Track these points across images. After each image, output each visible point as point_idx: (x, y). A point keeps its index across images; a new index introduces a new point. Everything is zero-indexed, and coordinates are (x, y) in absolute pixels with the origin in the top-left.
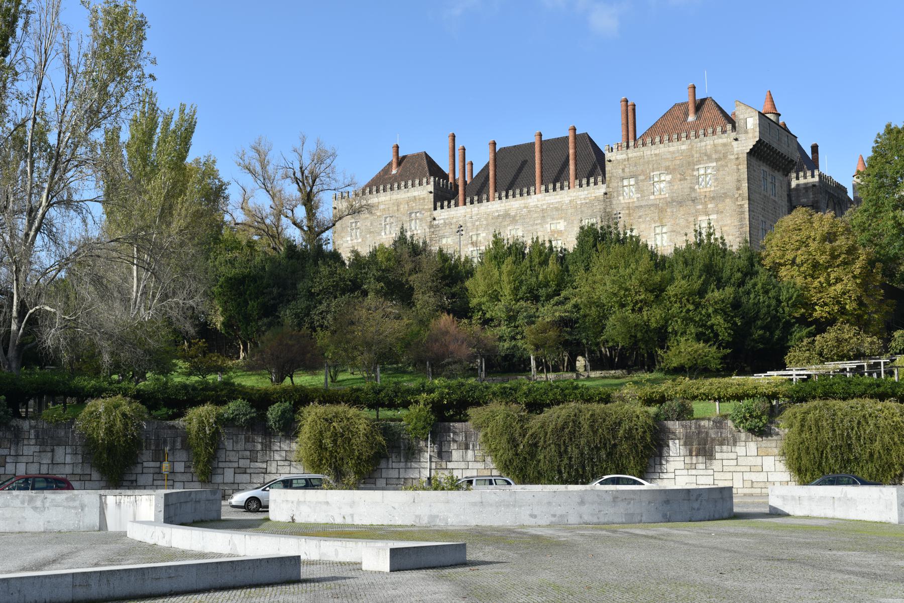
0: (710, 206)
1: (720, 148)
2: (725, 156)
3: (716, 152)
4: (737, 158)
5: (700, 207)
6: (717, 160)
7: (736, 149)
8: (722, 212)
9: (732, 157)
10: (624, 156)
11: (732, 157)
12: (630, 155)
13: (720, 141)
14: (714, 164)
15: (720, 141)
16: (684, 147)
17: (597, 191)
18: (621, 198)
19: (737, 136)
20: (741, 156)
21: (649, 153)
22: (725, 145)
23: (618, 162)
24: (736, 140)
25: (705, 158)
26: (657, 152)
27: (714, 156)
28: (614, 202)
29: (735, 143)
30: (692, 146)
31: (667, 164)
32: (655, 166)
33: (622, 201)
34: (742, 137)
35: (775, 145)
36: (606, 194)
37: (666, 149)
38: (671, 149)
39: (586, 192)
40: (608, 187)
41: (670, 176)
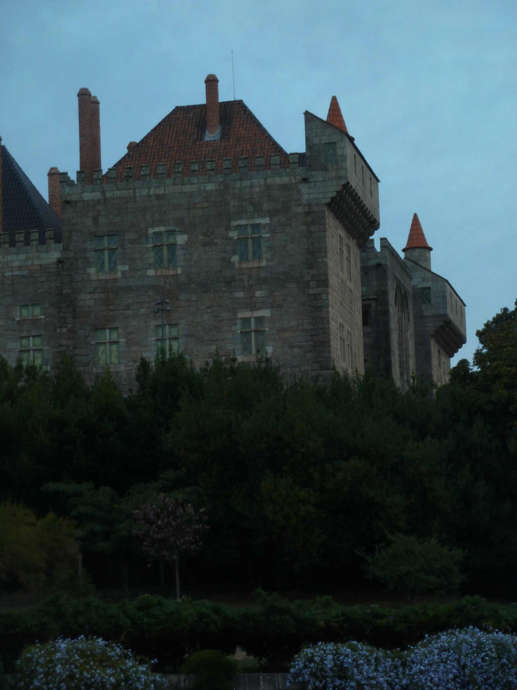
0: (258, 294)
4: (308, 213)
5: (240, 294)
6: (272, 214)
7: (305, 197)
8: (280, 306)
9: (299, 210)
10: (97, 195)
11: (299, 210)
12: (108, 195)
13: (278, 180)
14: (266, 221)
15: (278, 180)
16: (210, 187)
17: (44, 255)
18: (92, 271)
21: (145, 192)
22: (284, 187)
24: (305, 180)
25: (250, 209)
26: (161, 191)
27: (266, 206)
29: (304, 188)
33: (94, 277)
35: (360, 194)
36: (60, 262)
38: (187, 188)
39: (23, 257)
40: (66, 249)
41: (185, 237)
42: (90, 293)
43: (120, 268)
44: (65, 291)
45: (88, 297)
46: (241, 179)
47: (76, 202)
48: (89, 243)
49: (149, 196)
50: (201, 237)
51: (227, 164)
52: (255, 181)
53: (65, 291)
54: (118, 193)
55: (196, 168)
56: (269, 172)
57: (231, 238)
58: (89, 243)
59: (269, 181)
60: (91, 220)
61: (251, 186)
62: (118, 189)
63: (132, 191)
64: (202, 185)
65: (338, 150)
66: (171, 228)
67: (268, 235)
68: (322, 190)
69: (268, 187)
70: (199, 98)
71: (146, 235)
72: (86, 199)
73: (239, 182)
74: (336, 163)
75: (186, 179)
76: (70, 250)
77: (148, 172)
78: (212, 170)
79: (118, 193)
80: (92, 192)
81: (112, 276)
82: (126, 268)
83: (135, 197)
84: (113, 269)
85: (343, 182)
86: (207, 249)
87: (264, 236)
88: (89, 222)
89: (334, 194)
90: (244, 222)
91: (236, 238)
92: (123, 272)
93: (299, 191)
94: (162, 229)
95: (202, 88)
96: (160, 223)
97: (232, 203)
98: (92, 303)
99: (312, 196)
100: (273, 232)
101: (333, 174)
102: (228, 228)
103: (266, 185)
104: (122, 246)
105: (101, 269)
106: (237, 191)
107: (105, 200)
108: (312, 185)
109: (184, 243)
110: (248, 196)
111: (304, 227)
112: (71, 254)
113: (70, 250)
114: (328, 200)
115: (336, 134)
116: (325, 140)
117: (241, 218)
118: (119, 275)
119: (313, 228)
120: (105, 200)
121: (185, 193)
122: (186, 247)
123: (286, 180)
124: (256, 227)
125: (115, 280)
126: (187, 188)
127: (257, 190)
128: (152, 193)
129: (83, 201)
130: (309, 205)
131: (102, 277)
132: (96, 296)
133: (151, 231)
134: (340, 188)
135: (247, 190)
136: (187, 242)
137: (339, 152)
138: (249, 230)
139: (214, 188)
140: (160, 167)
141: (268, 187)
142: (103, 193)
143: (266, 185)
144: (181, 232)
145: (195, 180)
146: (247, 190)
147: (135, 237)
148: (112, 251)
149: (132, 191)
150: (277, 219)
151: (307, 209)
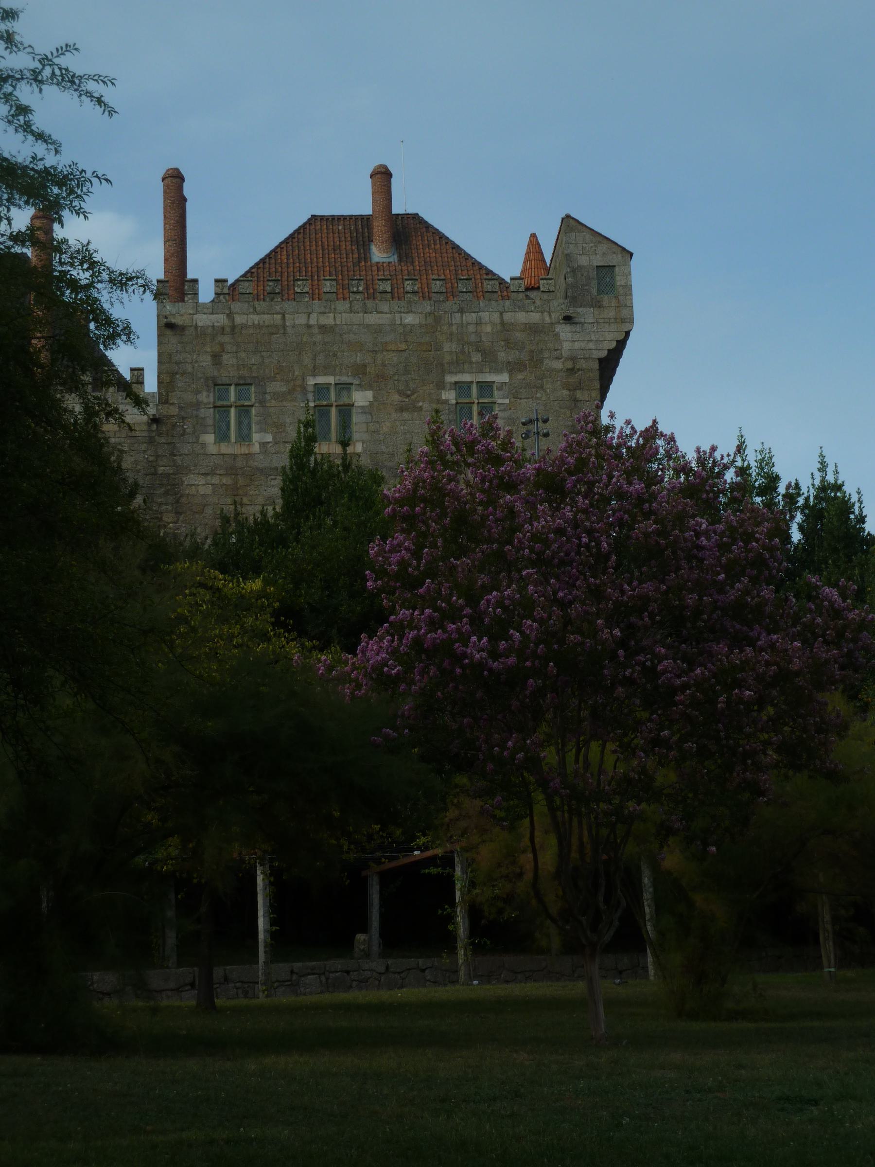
1: (519, 336)
2: (536, 361)
3: (509, 344)
4: (571, 371)
6: (513, 368)
7: (566, 346)
9: (558, 365)
11: (558, 365)
12: (239, 320)
13: (521, 317)
14: (504, 378)
15: (521, 317)
16: (409, 319)
19: (571, 312)
20: (582, 364)
21: (301, 320)
22: (533, 329)
23: (201, 333)
24: (568, 319)
25: (476, 357)
26: (328, 320)
27: (502, 356)
28: (186, 449)
29: (565, 331)
30: (438, 320)
31: (359, 358)
32: (321, 359)
33: (212, 449)
37: (357, 318)
38: (372, 319)
41: (369, 395)
42: (205, 474)
43: (256, 437)
44: (161, 469)
45: (201, 480)
46: (461, 311)
47: (183, 328)
48: (205, 394)
49: (309, 326)
50: (396, 397)
51: (437, 286)
52: (485, 316)
53: (161, 469)
54: (256, 318)
55: (389, 289)
56: (507, 303)
57: (446, 402)
58: (205, 394)
59: (507, 317)
60: (209, 358)
61: (479, 323)
62: (255, 311)
63: (279, 316)
64: (397, 316)
65: (618, 278)
66: (344, 379)
67: (507, 401)
68: (593, 338)
70: (359, 202)
71: (304, 388)
72: (200, 324)
73: (458, 315)
74: (616, 297)
75: (370, 304)
76: (173, 404)
77: (306, 289)
78: (414, 292)
79: (256, 318)
80: (212, 313)
81: (244, 450)
82: (269, 438)
83: (284, 326)
84: (244, 437)
86: (406, 415)
87: (499, 401)
88: (206, 360)
90: (466, 378)
91: (454, 402)
92: (263, 445)
93: (557, 335)
94: (331, 380)
95: (366, 187)
96: (327, 370)
97: (447, 347)
98: (209, 490)
99: (577, 345)
100: (515, 396)
101: (612, 314)
102: (441, 385)
103: (503, 323)
104: (262, 403)
105: (223, 437)
106: (454, 328)
107: (233, 327)
108: (578, 328)
109: (367, 404)
110: (473, 338)
111: (566, 392)
112: (174, 410)
113: (173, 404)
114: (604, 353)
115: (614, 253)
116: (598, 261)
117: (462, 372)
118: (256, 448)
119: (579, 395)
120: (233, 327)
121: (368, 326)
122: (367, 410)
123: (535, 317)
124: (486, 388)
125: (249, 455)
126: (372, 319)
127: (488, 329)
128: (312, 322)
129: (196, 327)
130: (573, 359)
131: (225, 449)
132: (215, 480)
133: (311, 381)
135: (471, 329)
136: (371, 404)
137: (619, 281)
138: (474, 390)
139: (417, 322)
140: (328, 283)
142: (230, 315)
143: (503, 323)
144: (360, 387)
145: (385, 307)
146: (471, 329)
147: (284, 389)
148: (244, 411)
149: (279, 316)
150: (520, 376)
151: (569, 365)
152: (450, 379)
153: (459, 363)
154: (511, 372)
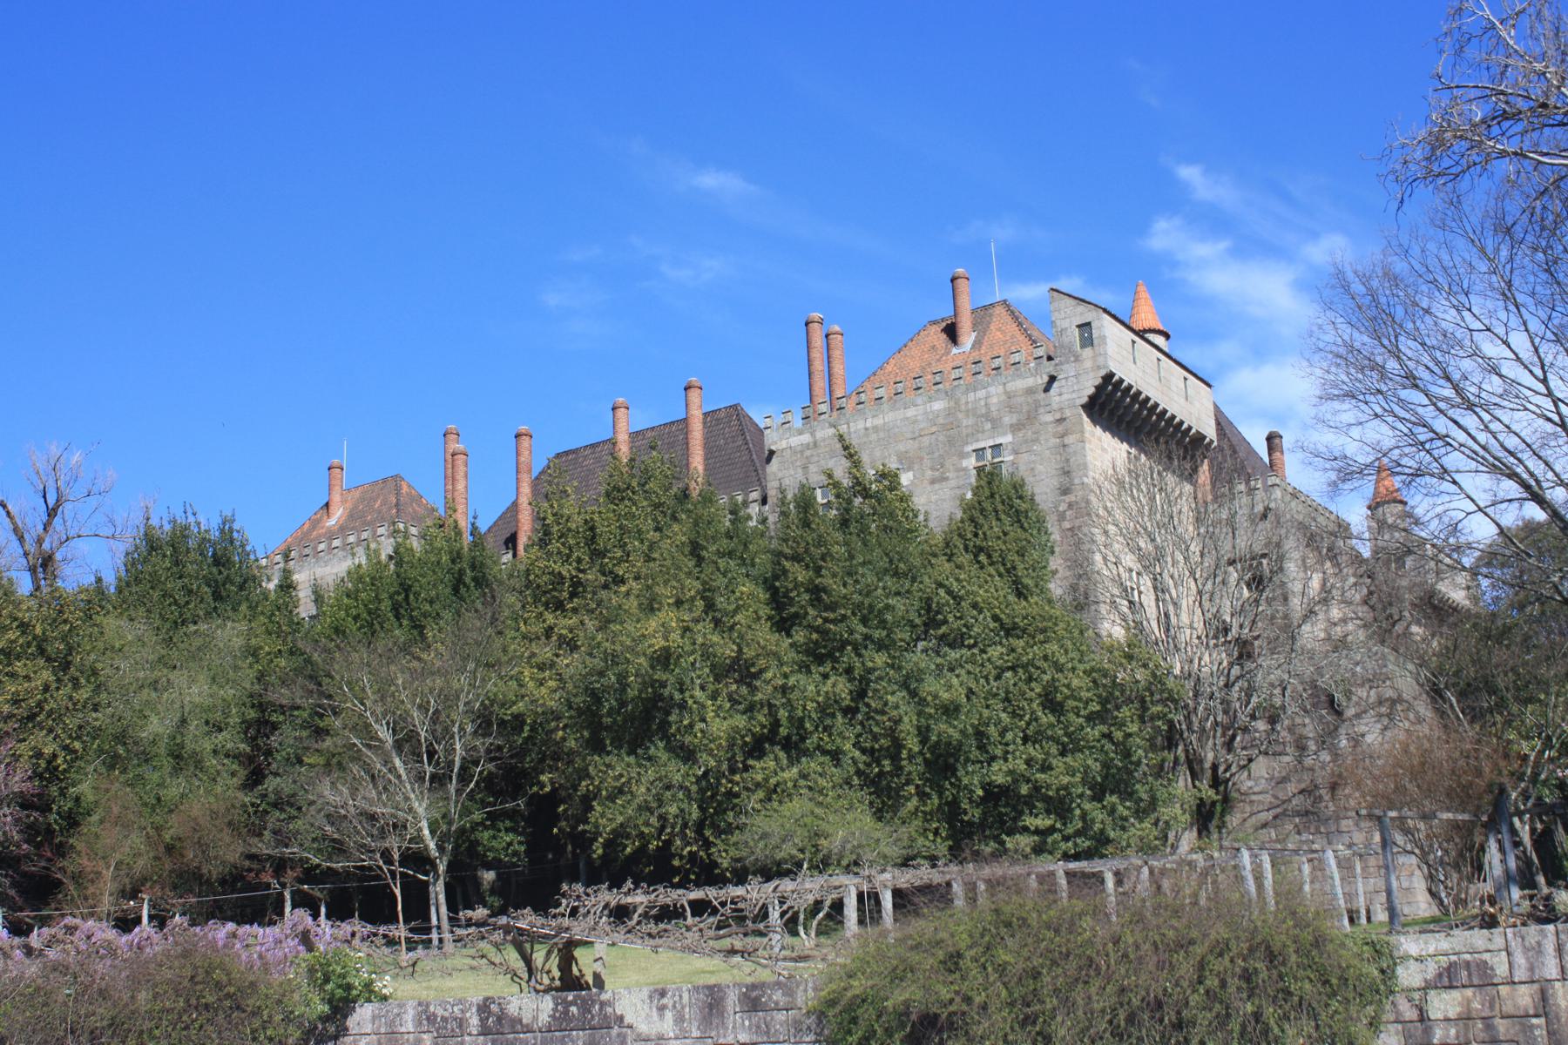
1: (1020, 400)
3: (1011, 409)
4: (1061, 420)
6: (1015, 428)
11: (1049, 418)
12: (819, 435)
21: (861, 425)
26: (879, 421)
34: (1067, 371)
69: (1009, 395)
85: (1103, 372)
86: (937, 486)
89: (1092, 390)
102: (963, 455)
114: (1085, 399)
124: (996, 448)
126: (911, 412)
127: (995, 400)
134: (1099, 381)
141: (1009, 395)
142: (813, 434)
143: (1006, 392)
151: (1058, 416)
152: (969, 448)
153: (977, 431)
154: (1013, 432)
